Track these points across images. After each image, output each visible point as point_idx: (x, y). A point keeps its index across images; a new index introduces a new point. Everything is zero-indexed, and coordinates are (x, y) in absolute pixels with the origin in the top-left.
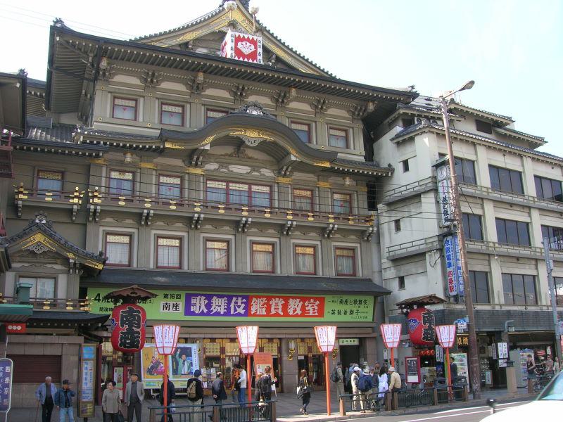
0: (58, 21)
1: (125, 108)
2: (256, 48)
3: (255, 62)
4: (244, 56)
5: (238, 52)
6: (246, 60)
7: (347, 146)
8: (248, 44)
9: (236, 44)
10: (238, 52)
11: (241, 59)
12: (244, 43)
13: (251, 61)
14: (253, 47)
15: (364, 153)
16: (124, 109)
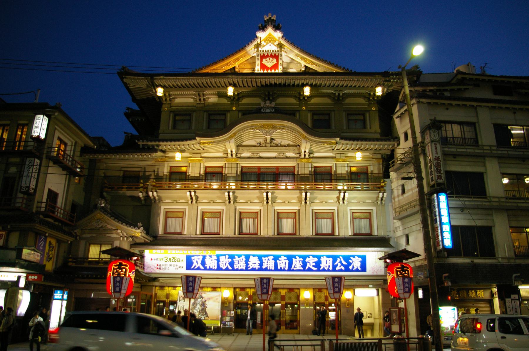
0: (124, 68)
1: (183, 121)
2: (277, 61)
3: (277, 71)
4: (268, 68)
5: (263, 66)
6: (269, 71)
7: (365, 127)
8: (271, 59)
9: (261, 61)
10: (263, 66)
11: (265, 71)
12: (268, 59)
13: (273, 71)
14: (275, 61)
15: (379, 130)
16: (183, 122)
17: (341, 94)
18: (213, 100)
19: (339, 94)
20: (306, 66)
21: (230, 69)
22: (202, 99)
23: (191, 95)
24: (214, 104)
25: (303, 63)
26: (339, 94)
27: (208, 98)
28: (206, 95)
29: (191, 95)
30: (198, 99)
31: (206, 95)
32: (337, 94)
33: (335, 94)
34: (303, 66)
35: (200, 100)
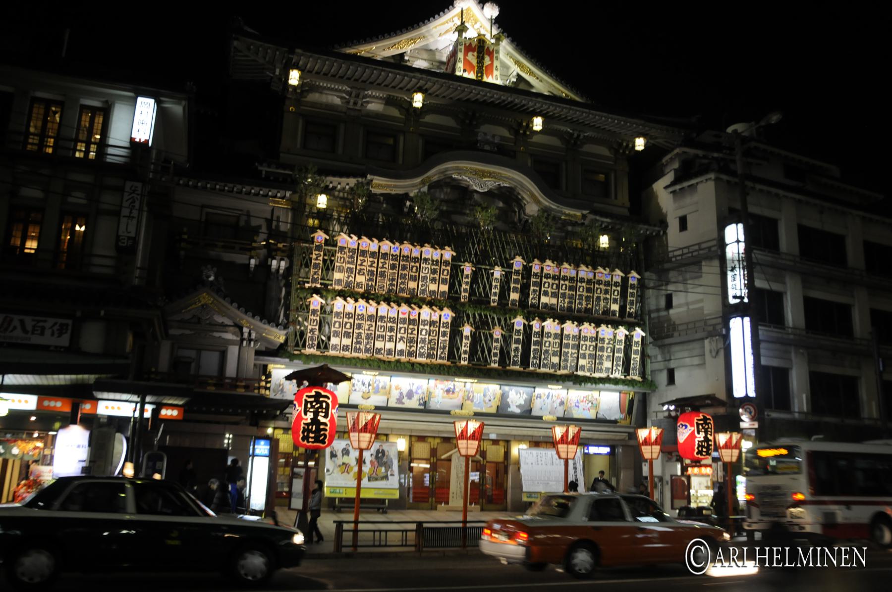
17: (582, 137)
18: (375, 106)
19: (579, 136)
20: (518, 75)
21: (393, 57)
22: (360, 102)
23: (340, 91)
24: (377, 115)
25: (515, 70)
26: (579, 136)
27: (368, 102)
28: (365, 96)
29: (340, 91)
30: (352, 101)
31: (365, 96)
32: (575, 135)
33: (572, 135)
34: (515, 74)
35: (355, 103)
